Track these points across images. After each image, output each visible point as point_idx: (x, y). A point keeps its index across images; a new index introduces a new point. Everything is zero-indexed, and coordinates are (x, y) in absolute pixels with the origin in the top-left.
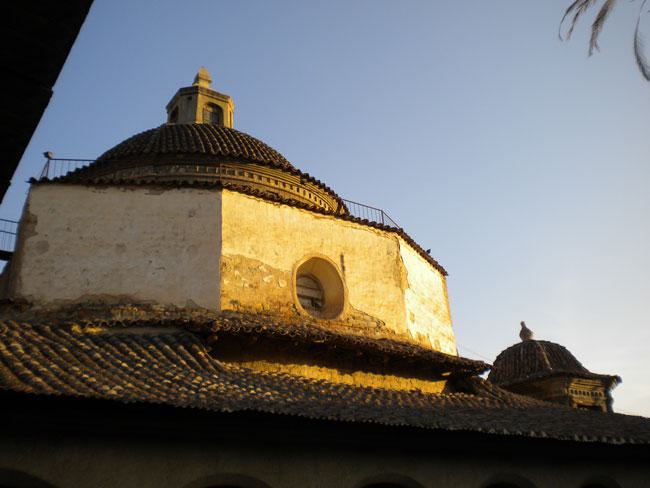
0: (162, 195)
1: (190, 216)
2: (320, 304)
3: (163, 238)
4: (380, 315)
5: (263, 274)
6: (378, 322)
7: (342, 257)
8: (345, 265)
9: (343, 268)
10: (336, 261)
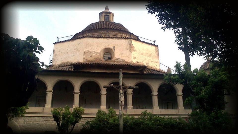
0: (74, 41)
1: (79, 44)
2: (111, 58)
3: (74, 50)
4: (123, 58)
5: (93, 53)
6: (123, 60)
7: (114, 47)
8: (115, 48)
9: (114, 49)
10: (112, 48)
